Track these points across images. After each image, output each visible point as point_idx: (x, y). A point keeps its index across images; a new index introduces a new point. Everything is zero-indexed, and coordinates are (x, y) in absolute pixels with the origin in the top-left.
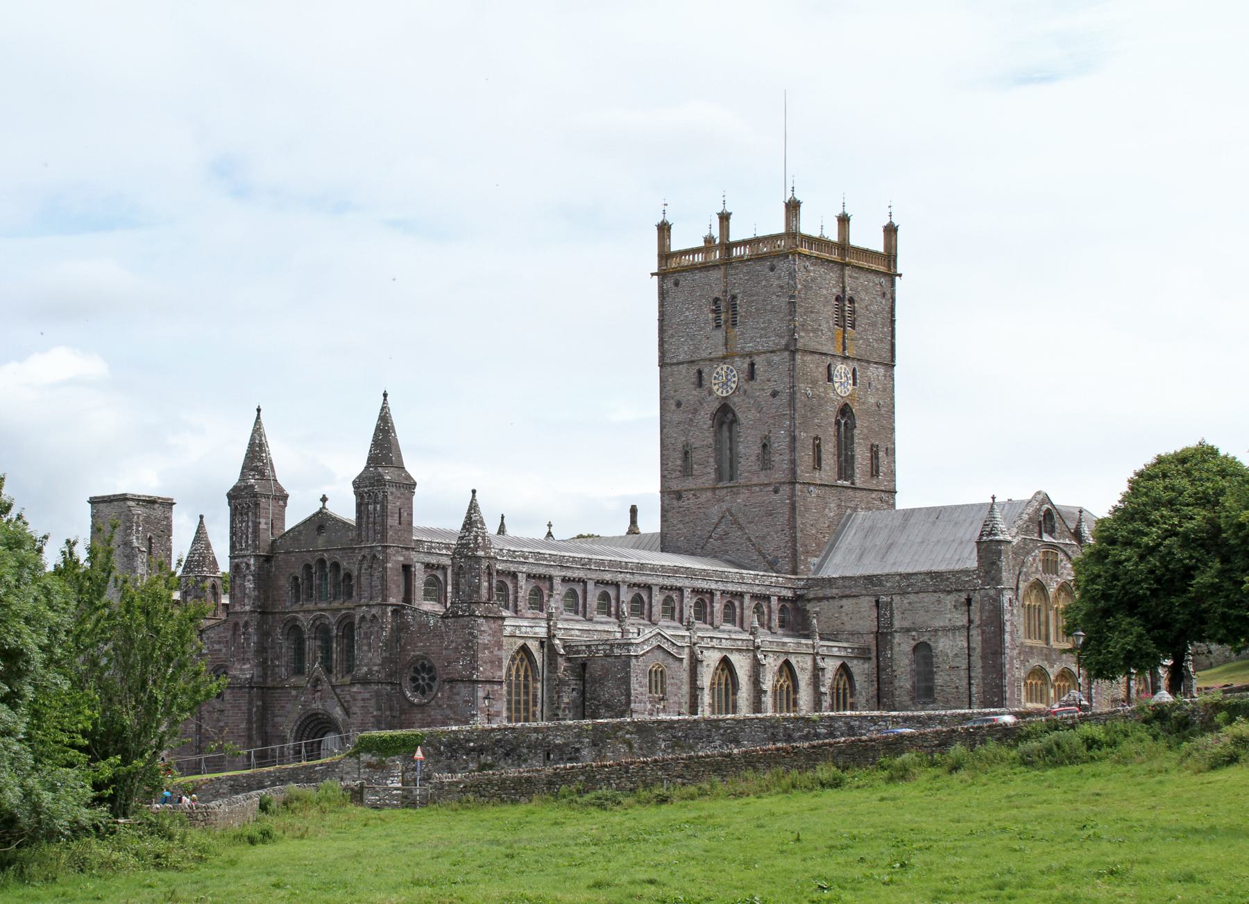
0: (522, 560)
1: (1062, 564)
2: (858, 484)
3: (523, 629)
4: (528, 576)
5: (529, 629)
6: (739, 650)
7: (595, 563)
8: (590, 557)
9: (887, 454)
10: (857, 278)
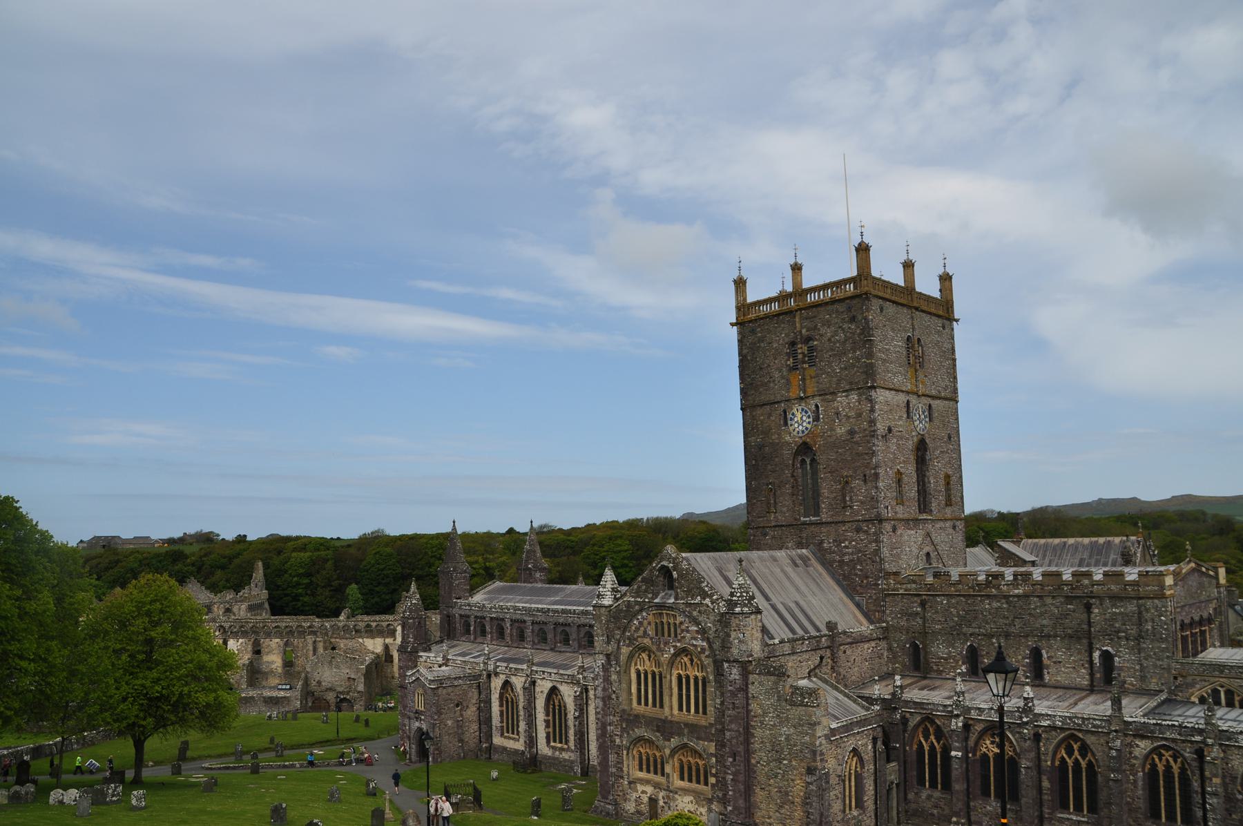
0: (506, 611)
1: (683, 627)
2: (825, 517)
3: (431, 658)
4: (511, 620)
5: (434, 659)
6: (566, 682)
7: (552, 611)
8: (549, 607)
9: (865, 481)
10: (815, 317)
